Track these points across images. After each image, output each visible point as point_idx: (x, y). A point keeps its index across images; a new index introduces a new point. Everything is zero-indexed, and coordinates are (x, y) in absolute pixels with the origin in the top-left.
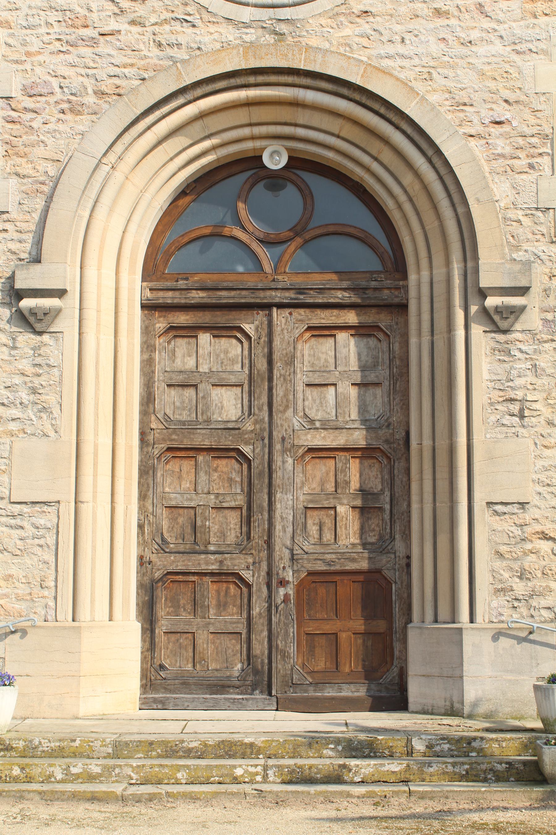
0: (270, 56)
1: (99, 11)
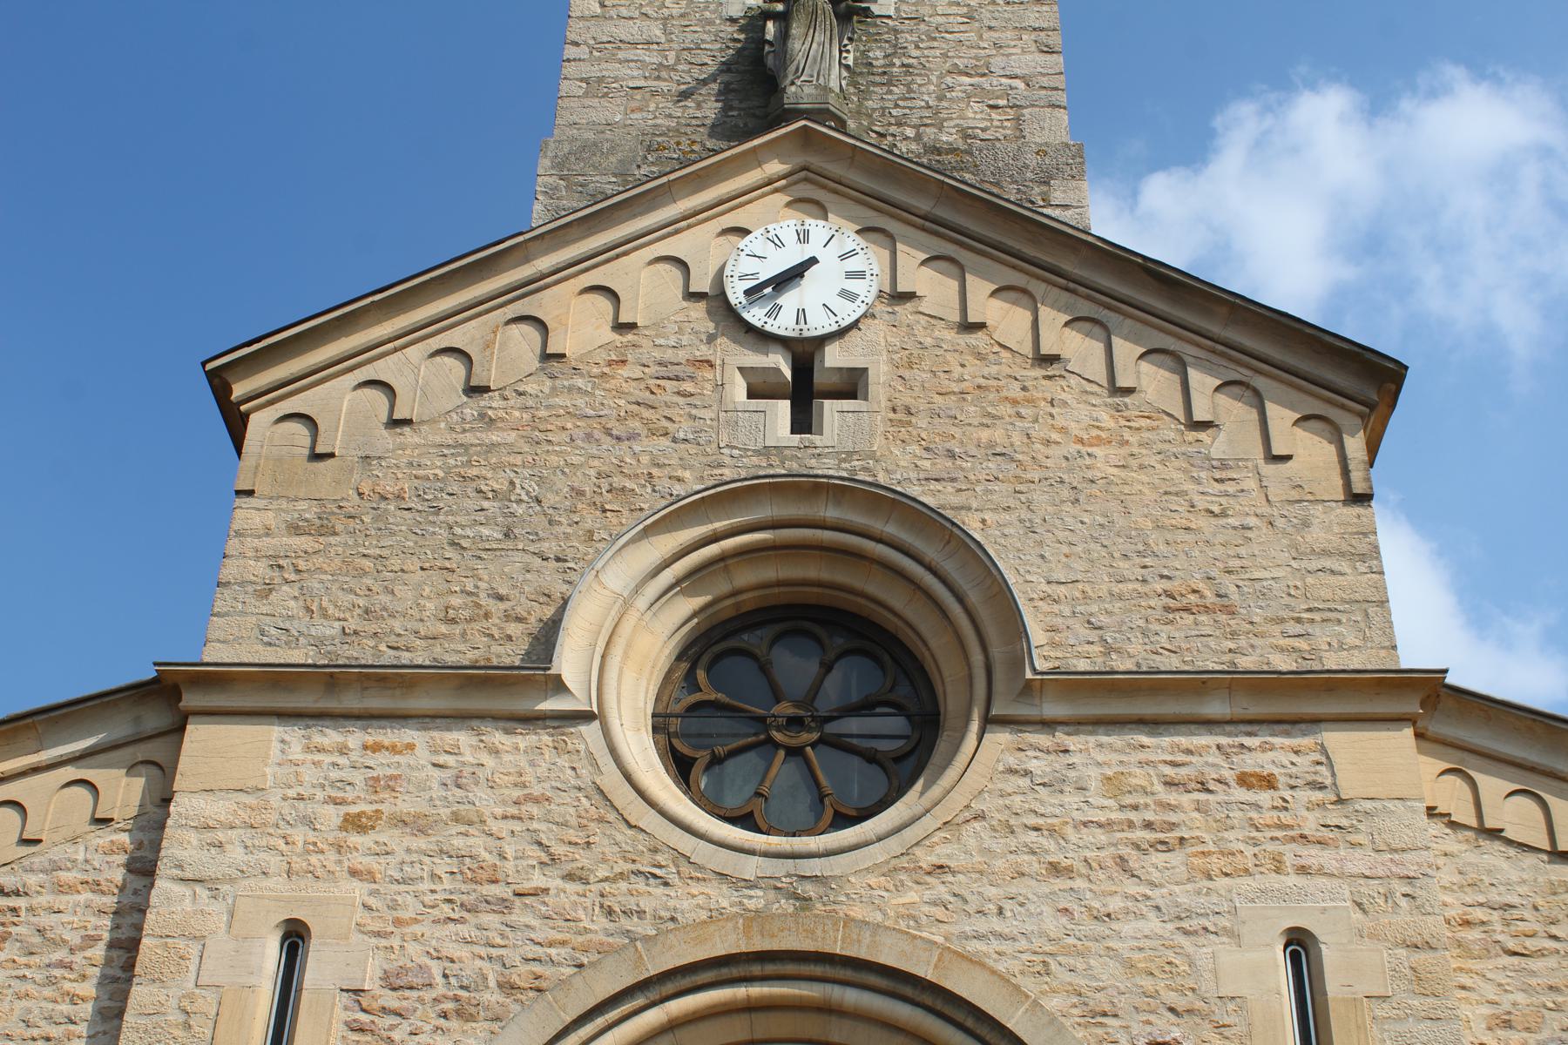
1: (516, 858)
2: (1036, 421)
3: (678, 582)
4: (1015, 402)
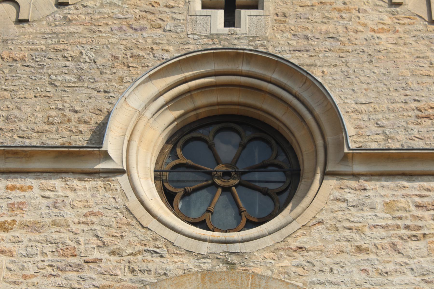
0: (222, 281)
1: (85, 244)
2: (350, 20)
3: (167, 104)
4: (340, 10)
